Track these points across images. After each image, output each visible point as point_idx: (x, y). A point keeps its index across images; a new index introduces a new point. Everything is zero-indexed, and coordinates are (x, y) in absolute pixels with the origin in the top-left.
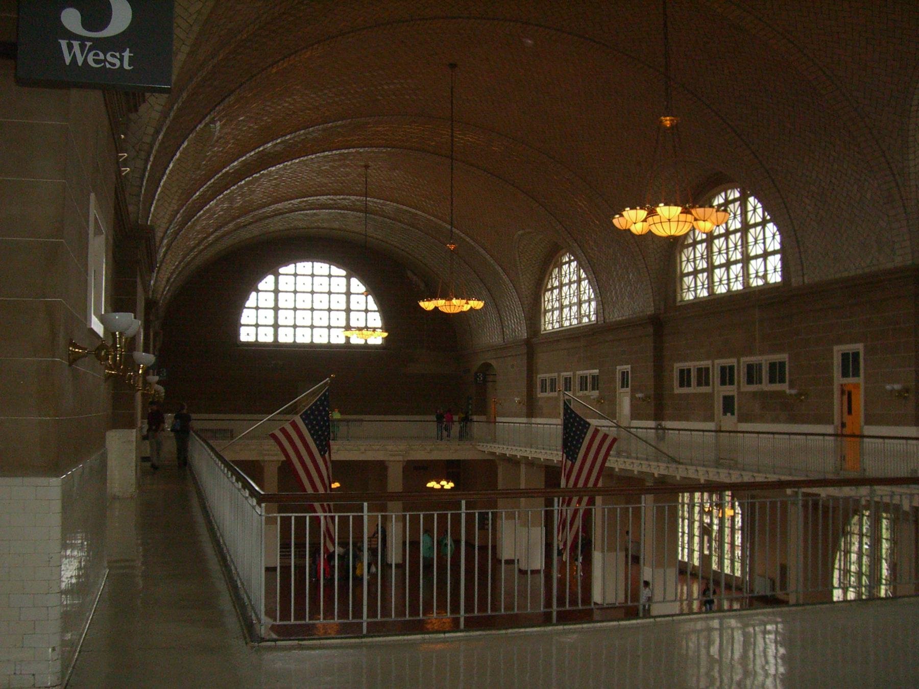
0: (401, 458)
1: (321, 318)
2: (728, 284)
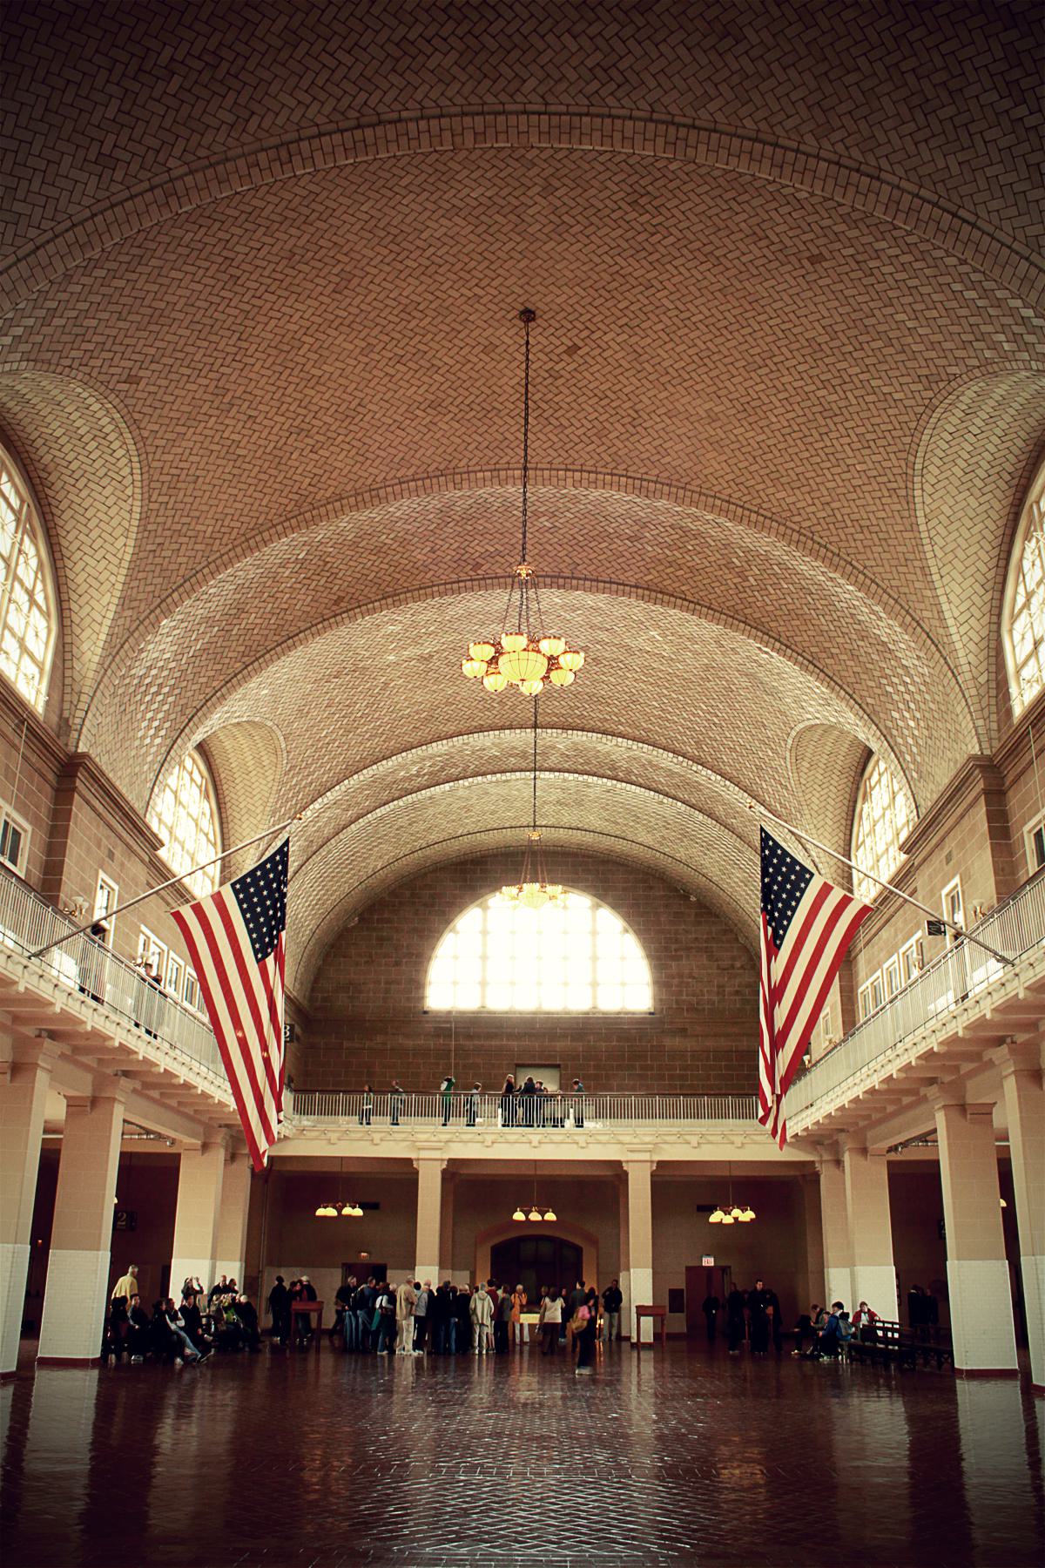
0: (646, 1157)
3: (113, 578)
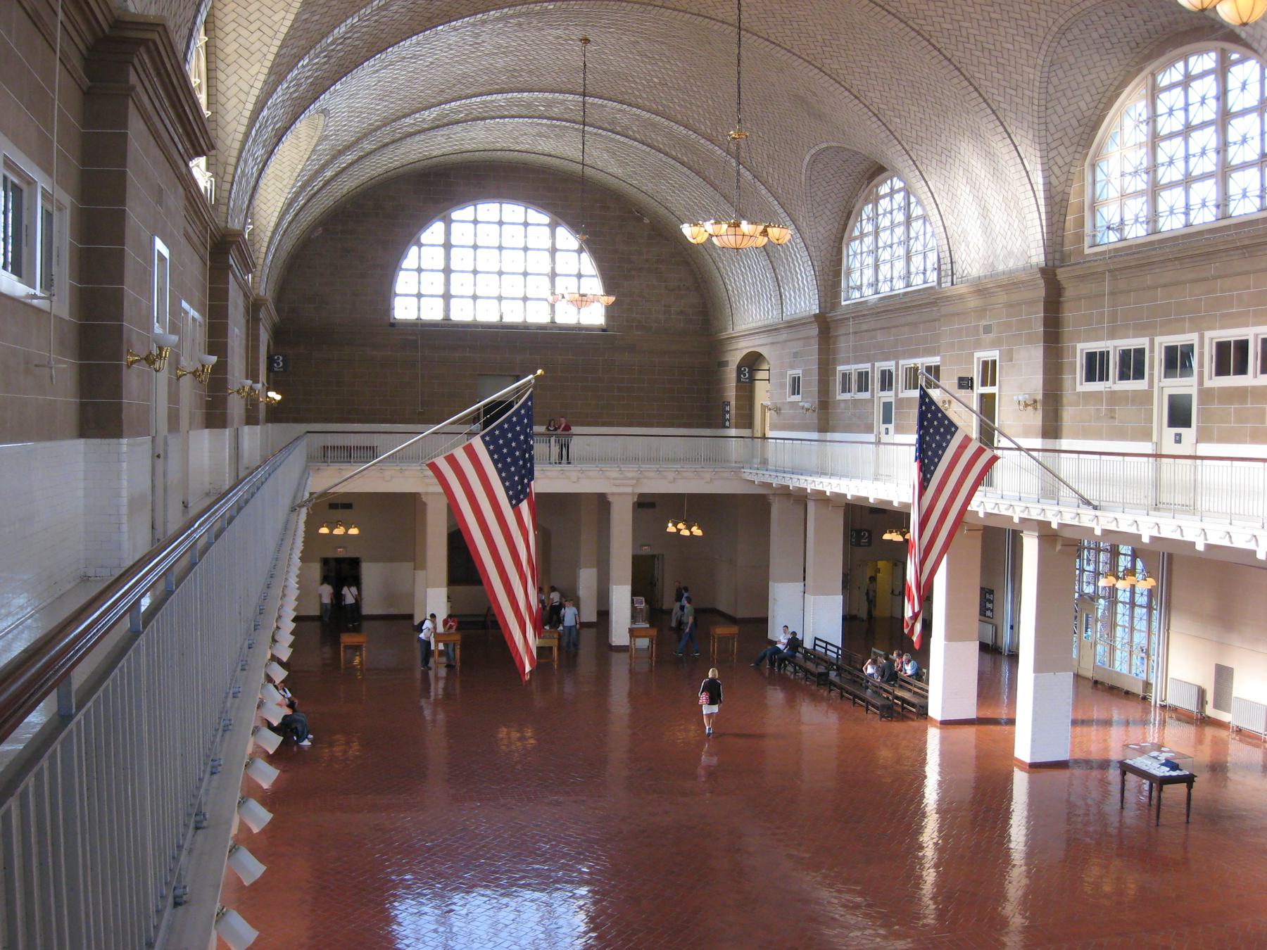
0: (629, 490)
1: (513, 286)
2: (1187, 214)
3: (265, 49)
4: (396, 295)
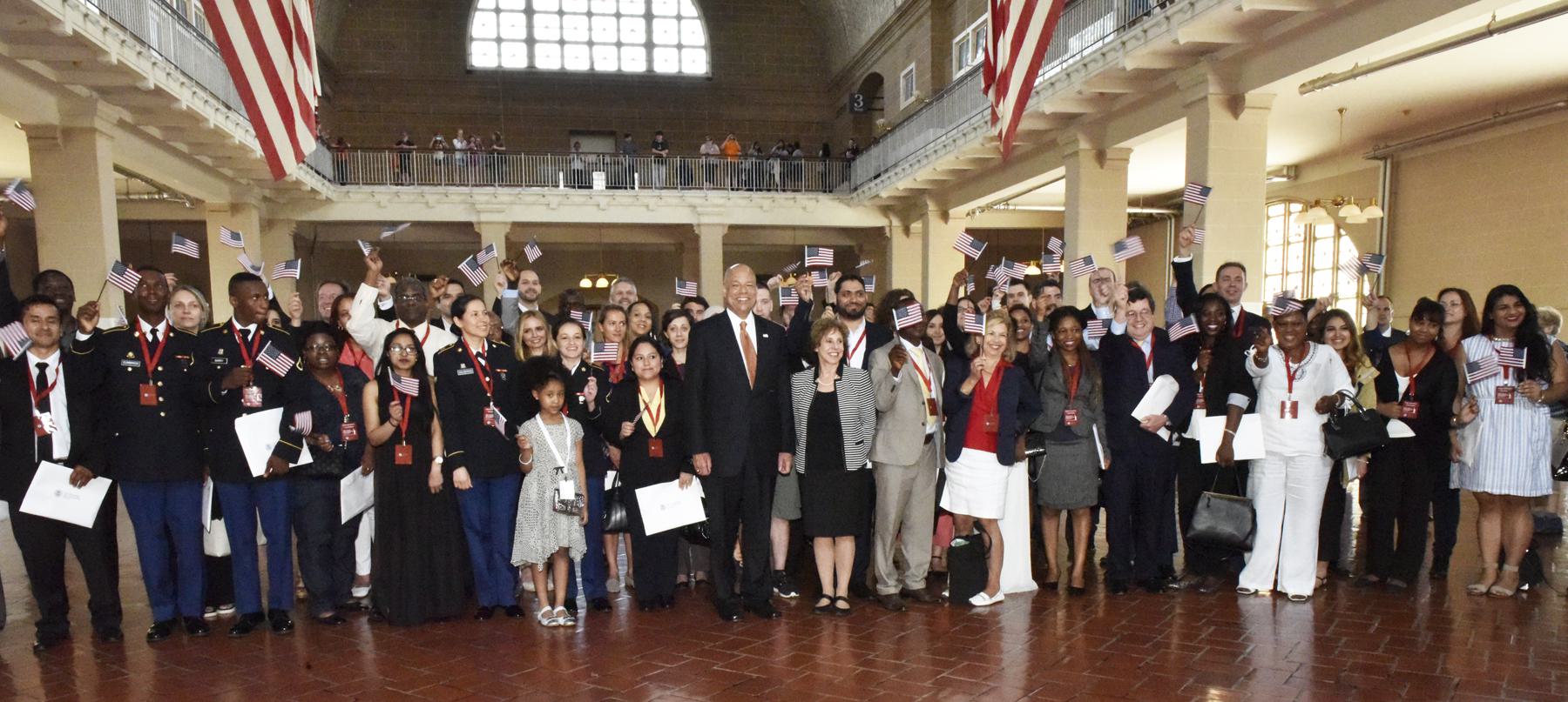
4: (472, 39)
